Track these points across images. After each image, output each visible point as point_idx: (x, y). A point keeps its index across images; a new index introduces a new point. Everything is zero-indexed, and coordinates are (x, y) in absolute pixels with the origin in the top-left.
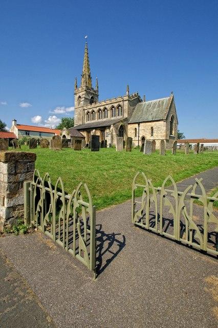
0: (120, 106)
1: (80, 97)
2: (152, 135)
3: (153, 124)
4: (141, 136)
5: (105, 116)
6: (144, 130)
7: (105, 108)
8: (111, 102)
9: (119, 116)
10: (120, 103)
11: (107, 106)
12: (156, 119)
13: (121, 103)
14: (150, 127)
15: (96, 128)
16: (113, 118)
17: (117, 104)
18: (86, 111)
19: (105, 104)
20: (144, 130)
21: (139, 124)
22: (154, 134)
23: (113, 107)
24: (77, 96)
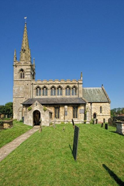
0: (74, 87)
1: (22, 70)
2: (101, 112)
3: (102, 104)
4: (93, 113)
5: (58, 93)
6: (95, 108)
7: (60, 87)
8: (66, 83)
9: (73, 95)
10: (75, 85)
11: (62, 85)
12: (103, 101)
13: (77, 85)
14: (99, 107)
15: (68, 105)
16: (68, 97)
17: (73, 85)
18: (36, 86)
19: (59, 83)
20: (95, 108)
21: (91, 104)
22: (103, 112)
23: (68, 87)
24: (18, 68)
